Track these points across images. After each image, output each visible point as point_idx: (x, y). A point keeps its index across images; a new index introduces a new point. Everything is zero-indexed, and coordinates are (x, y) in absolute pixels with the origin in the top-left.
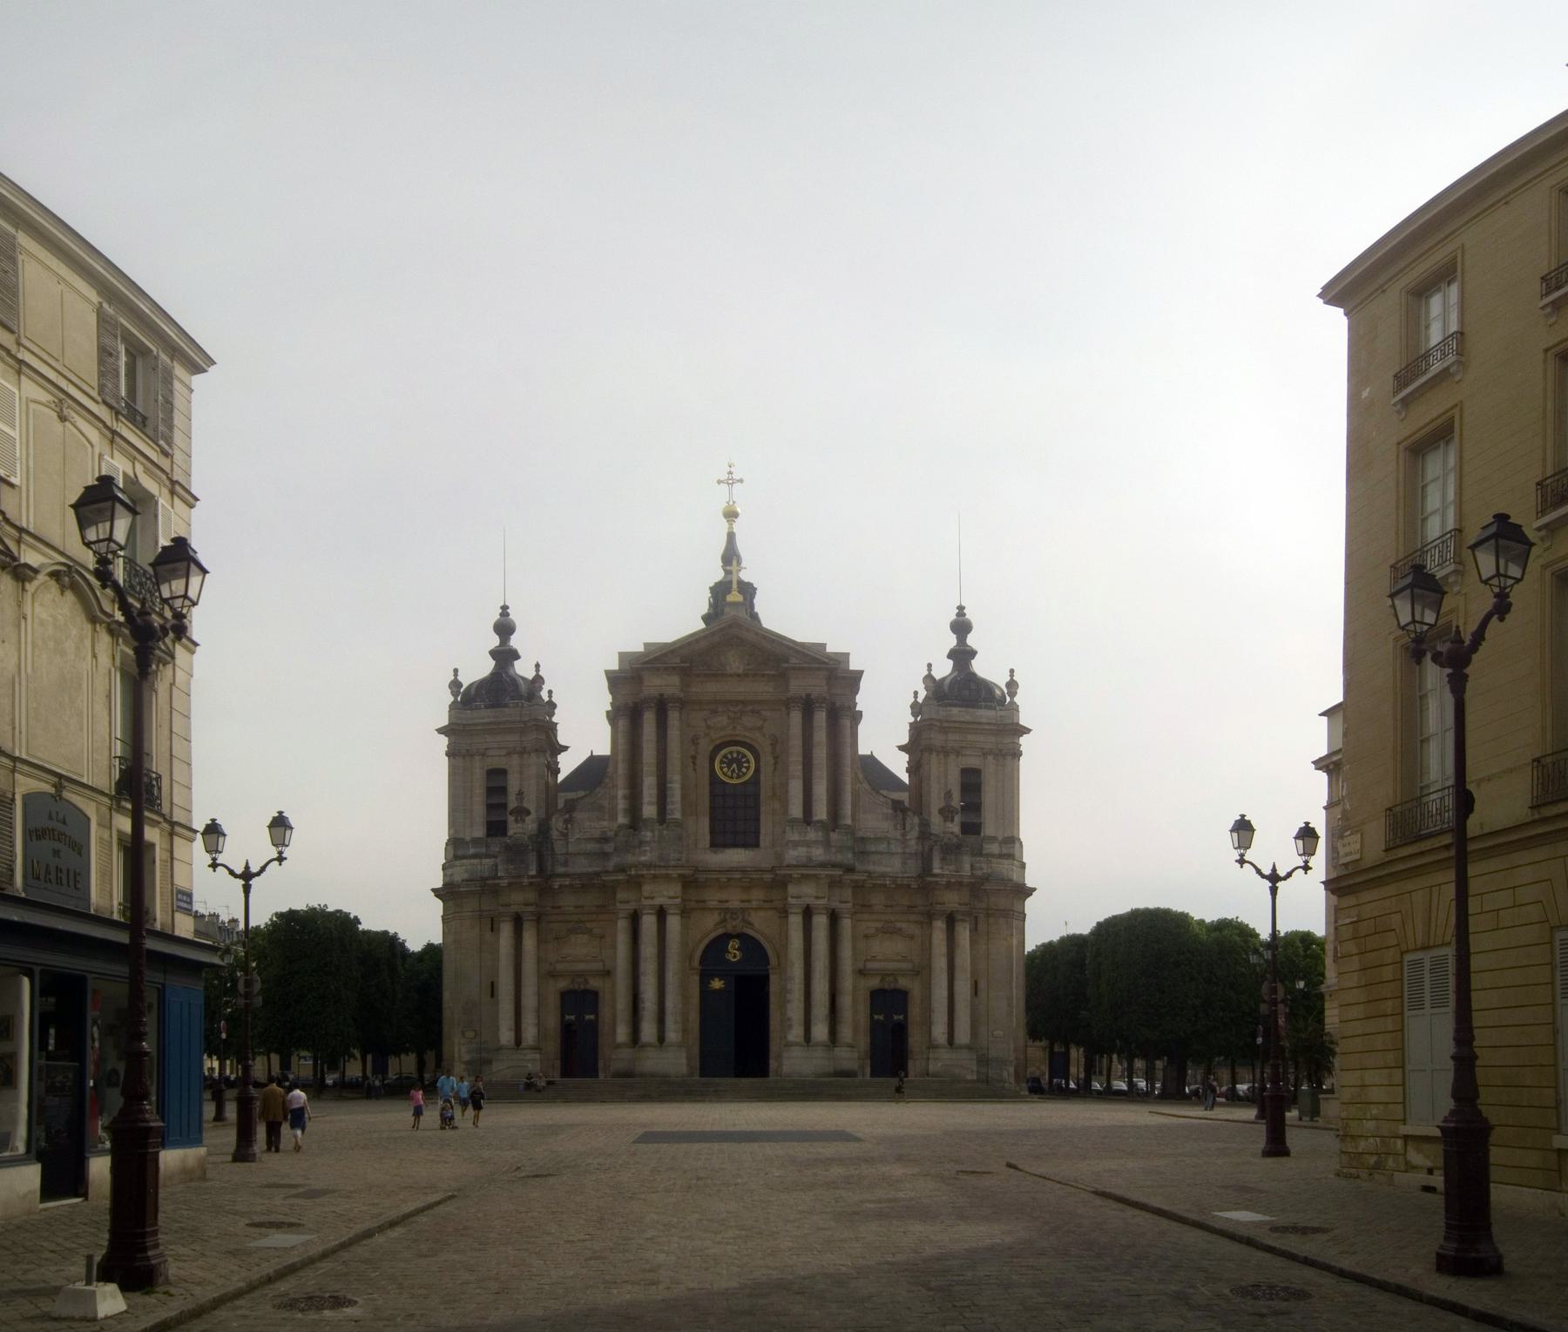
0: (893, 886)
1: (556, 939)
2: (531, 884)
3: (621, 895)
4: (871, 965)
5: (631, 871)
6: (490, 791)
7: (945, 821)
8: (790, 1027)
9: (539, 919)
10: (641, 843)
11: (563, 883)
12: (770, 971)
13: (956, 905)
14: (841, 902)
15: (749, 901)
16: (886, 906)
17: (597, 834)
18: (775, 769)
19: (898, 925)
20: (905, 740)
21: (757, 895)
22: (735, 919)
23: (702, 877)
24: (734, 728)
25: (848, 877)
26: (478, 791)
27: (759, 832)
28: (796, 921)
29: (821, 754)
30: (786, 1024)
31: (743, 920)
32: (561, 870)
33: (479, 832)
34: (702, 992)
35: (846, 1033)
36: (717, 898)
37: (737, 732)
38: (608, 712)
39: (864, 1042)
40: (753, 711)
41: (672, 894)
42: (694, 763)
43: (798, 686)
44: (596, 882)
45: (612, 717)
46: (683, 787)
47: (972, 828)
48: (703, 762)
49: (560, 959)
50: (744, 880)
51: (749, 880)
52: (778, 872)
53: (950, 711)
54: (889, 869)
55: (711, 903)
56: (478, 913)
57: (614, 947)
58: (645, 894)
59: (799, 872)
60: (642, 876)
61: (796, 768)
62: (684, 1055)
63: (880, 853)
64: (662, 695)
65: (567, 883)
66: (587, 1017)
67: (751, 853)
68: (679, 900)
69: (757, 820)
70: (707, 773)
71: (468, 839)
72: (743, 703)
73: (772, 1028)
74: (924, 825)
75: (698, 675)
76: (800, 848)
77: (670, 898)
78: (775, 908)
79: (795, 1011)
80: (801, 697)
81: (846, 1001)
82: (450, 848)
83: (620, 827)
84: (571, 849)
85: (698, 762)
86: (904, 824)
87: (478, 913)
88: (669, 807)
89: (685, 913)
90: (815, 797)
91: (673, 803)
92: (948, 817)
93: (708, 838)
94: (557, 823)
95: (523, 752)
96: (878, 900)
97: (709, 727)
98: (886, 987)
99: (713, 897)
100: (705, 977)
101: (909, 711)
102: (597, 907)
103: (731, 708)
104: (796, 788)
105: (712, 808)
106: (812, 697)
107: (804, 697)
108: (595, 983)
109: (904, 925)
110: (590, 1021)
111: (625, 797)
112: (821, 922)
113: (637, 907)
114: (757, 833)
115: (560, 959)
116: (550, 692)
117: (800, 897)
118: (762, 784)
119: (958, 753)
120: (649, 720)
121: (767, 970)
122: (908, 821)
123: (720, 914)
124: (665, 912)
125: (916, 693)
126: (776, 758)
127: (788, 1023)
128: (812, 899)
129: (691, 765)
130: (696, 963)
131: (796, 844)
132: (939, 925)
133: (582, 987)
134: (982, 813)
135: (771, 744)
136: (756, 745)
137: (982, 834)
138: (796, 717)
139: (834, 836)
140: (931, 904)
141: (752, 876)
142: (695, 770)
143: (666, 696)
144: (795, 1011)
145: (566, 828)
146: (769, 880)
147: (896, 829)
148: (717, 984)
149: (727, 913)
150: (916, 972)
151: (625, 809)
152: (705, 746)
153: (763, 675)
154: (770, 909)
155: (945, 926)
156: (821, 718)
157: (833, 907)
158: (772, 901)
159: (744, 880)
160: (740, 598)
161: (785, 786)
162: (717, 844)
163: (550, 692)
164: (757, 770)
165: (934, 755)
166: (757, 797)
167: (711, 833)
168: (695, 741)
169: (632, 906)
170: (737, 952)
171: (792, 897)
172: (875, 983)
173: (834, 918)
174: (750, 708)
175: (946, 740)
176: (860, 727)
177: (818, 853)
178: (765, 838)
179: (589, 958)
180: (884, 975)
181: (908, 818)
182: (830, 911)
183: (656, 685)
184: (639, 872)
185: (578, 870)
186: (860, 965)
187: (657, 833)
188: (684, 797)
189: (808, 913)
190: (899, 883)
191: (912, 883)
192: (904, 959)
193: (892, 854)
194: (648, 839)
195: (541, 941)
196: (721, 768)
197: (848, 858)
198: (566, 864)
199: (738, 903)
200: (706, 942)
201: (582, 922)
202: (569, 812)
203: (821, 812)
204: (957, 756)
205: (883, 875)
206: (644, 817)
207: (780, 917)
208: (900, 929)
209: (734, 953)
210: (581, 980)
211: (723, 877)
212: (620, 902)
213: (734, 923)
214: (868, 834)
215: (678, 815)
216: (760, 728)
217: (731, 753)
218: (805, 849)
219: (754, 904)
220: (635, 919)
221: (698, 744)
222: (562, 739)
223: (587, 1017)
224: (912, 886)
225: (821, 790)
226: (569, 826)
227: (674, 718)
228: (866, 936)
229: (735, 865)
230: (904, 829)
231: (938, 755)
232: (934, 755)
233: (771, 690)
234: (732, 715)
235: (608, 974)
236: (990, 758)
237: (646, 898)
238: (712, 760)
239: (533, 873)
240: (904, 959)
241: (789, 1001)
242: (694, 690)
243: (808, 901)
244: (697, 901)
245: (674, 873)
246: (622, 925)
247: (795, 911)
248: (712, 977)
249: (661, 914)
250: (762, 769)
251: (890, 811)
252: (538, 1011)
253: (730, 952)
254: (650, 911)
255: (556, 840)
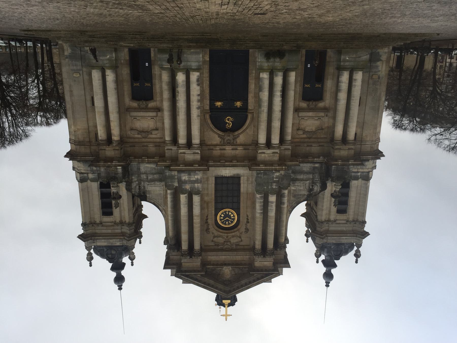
0: (143, 158)
1: (322, 129)
2: (336, 160)
3: (289, 153)
4: (154, 114)
5: (285, 168)
6: (345, 203)
7: (118, 193)
8: (198, 80)
9: (332, 140)
10: (277, 182)
11: (317, 159)
12: (209, 111)
13: (107, 149)
14: (171, 149)
15: (221, 149)
16: (147, 146)
17: (297, 183)
18: (207, 217)
19: (139, 136)
20: (144, 221)
21: (217, 152)
22: (229, 140)
23: (246, 163)
24: (227, 237)
25: (168, 163)
26: (352, 203)
27: (215, 184)
28: (196, 140)
29: (184, 228)
30: (200, 82)
31: (224, 139)
32: (317, 165)
33: (354, 183)
34: (247, 100)
35: (165, 77)
36: (238, 151)
37: (226, 235)
38: (288, 243)
39: (156, 70)
40: (218, 245)
41: (263, 155)
42: (248, 219)
43: (196, 262)
44: (301, 159)
45: (287, 241)
46: (254, 208)
47: (105, 186)
48: (243, 220)
49: (322, 119)
50: (224, 161)
51: (221, 161)
52: (206, 167)
53: (120, 244)
54: (147, 165)
55: (241, 148)
56: (362, 143)
57: (293, 124)
58: (278, 155)
59: (196, 168)
60: (279, 165)
61: (197, 220)
62: (258, 64)
63: (153, 174)
64: (264, 257)
65: (315, 159)
66: (309, 86)
67: (219, 174)
68: (259, 152)
69: (216, 190)
70: (241, 215)
71: (360, 180)
72: (222, 250)
73: (208, 79)
74: (129, 189)
75: (245, 264)
76: (194, 179)
77: (264, 153)
78: (207, 145)
79: (195, 90)
80: (194, 255)
81: (166, 95)
82: (370, 176)
83: (286, 189)
84: (311, 176)
85: (245, 220)
86: (140, 189)
87: (362, 143)
88: (262, 200)
89: (256, 143)
90: (186, 206)
91: (261, 202)
92: (116, 195)
93: (242, 182)
94: (317, 188)
95: (328, 221)
96: (152, 149)
97: (240, 237)
98: (144, 103)
99: (240, 151)
100: (245, 108)
101: (143, 234)
102: (299, 146)
103: (229, 247)
104: (197, 210)
105: (239, 196)
106: (189, 257)
107: (193, 257)
108: (304, 105)
109: (137, 136)
110: (307, 84)
111: (284, 203)
112: (182, 140)
113: (281, 146)
114: (216, 184)
115: (322, 119)
116: (307, 241)
117: (194, 153)
118: (214, 209)
119: (115, 223)
120: (270, 244)
121: (211, 112)
122: (137, 190)
123: (236, 142)
124: (266, 145)
125: (140, 243)
126: (207, 222)
127: (199, 82)
128: (187, 152)
129: (249, 218)
130: (250, 116)
131: (197, 181)
132: (116, 137)
133: (311, 103)
134: (100, 194)
135: (209, 229)
136: (216, 228)
137: (99, 182)
138: (197, 246)
139: (176, 184)
140: (121, 149)
141: (219, 163)
142: (247, 216)
143: (262, 256)
144: (195, 90)
145: (312, 186)
146: (210, 161)
147: (144, 187)
148: (238, 104)
149: (232, 144)
150: (129, 109)
151: (284, 197)
152: (242, 227)
153: (213, 265)
154: (210, 145)
155: (113, 138)
156: (185, 246)
157: (175, 147)
158: (209, 149)
159: (224, 161)
160: (224, 301)
161: (202, 208)
162: (236, 179)
163: (307, 241)
164: (216, 215)
165: (127, 222)
166: (216, 202)
167: (240, 184)
168: (247, 230)
169: (283, 147)
170: (227, 121)
171: (198, 153)
172: (151, 104)
173: (175, 140)
174: (219, 247)
175: (121, 229)
176: (165, 236)
177: (185, 177)
178: (212, 181)
179: (305, 118)
180: (147, 109)
181: (137, 192)
182: (177, 145)
183: (267, 262)
184: (281, 167)
185: (309, 165)
186: (159, 114)
187: (270, 187)
188: (254, 203)
189: (189, 144)
190: (140, 160)
191: (133, 160)
192: (135, 118)
193: (145, 173)
194: (274, 184)
195: (332, 128)
196: (234, 216)
197: (168, 173)
198: (314, 168)
199: (227, 148)
200: (244, 127)
201: (309, 138)
202: (311, 194)
203: (183, 198)
204: (115, 221)
205: (149, 162)
206: (276, 195)
207: (205, 141)
208: (138, 134)
209: (229, 121)
210: (311, 107)
211: (235, 163)
212: (289, 149)
213: (229, 138)
214: (158, 183)
215: (258, 196)
216: (214, 237)
217: (229, 224)
218: (192, 179)
219: (218, 148)
220: (282, 140)
221: (245, 229)
222: (304, 219)
223: (309, 86)
224: (133, 158)
225: (184, 210)
226: (311, 187)
227: (258, 245)
228: (157, 129)
229: (228, 168)
230: (139, 187)
231: (126, 221)
232: (127, 222)
233: (209, 257)
234: (229, 243)
235: (297, 110)
236: (98, 221)
237: (277, 153)
238: (238, 220)
239: (333, 166)
240: (135, 118)
241: (198, 95)
242: (248, 257)
243: (187, 151)
244: (248, 149)
245: (262, 167)
246: (289, 138)
247: (195, 146)
248: (240, 108)
249: (269, 144)
250: (214, 216)
251: (148, 195)
252: (337, 90)
253: (231, 121)
254: (275, 145)
255: (318, 180)
